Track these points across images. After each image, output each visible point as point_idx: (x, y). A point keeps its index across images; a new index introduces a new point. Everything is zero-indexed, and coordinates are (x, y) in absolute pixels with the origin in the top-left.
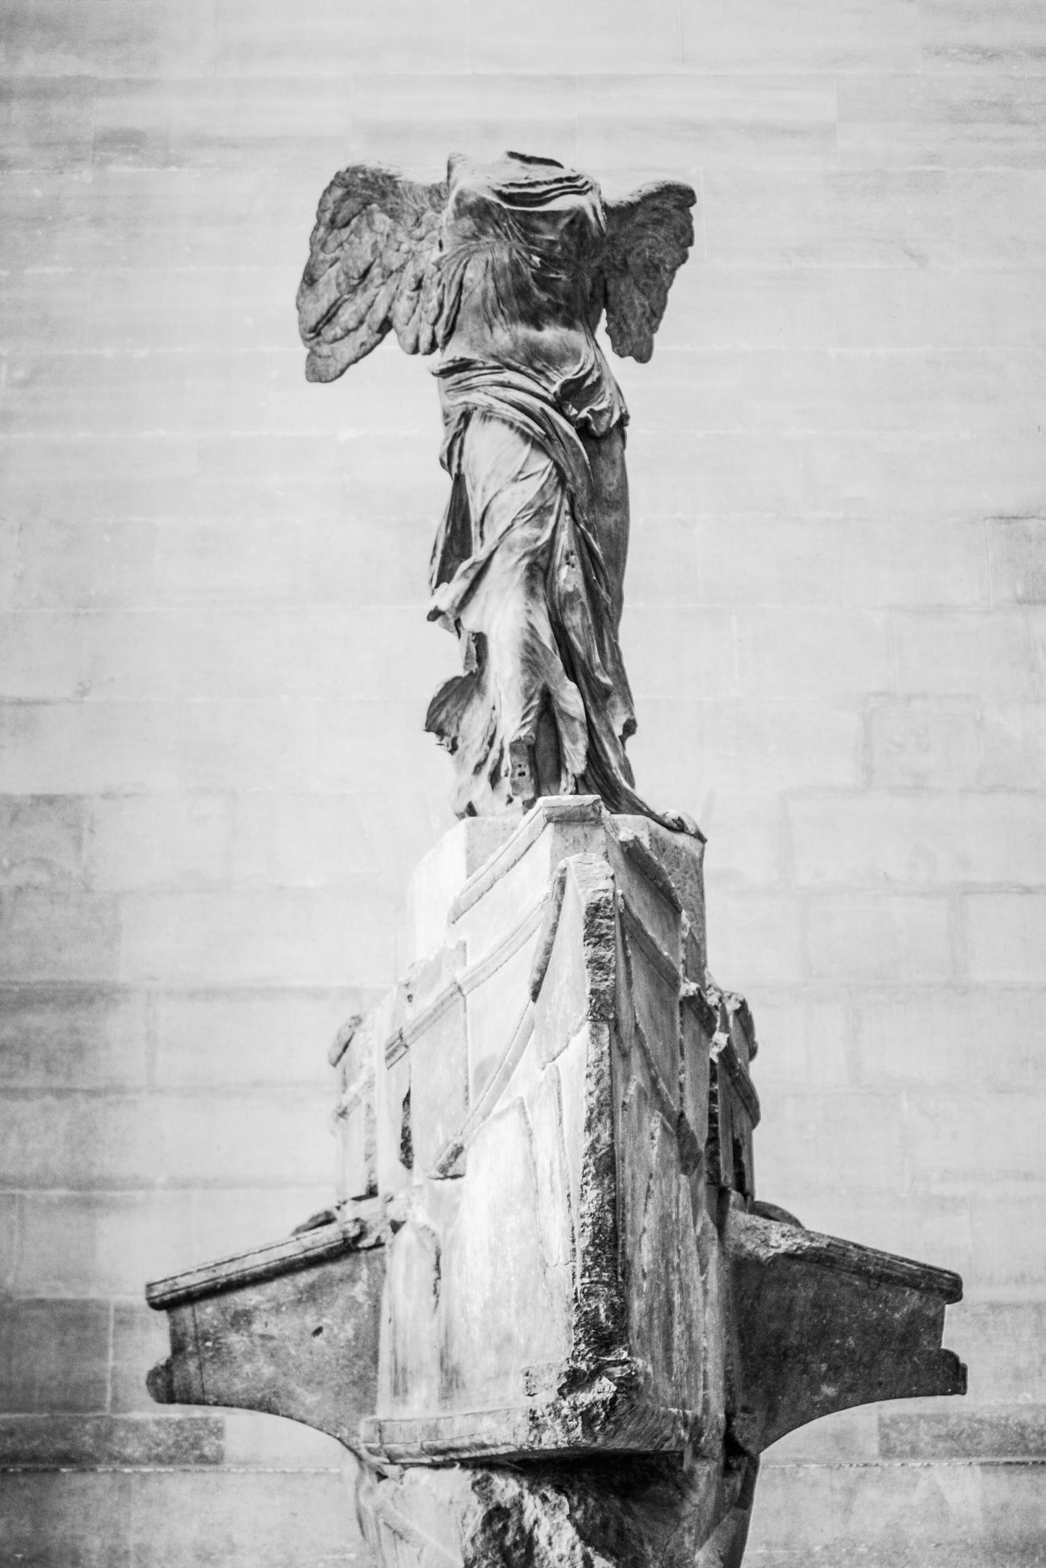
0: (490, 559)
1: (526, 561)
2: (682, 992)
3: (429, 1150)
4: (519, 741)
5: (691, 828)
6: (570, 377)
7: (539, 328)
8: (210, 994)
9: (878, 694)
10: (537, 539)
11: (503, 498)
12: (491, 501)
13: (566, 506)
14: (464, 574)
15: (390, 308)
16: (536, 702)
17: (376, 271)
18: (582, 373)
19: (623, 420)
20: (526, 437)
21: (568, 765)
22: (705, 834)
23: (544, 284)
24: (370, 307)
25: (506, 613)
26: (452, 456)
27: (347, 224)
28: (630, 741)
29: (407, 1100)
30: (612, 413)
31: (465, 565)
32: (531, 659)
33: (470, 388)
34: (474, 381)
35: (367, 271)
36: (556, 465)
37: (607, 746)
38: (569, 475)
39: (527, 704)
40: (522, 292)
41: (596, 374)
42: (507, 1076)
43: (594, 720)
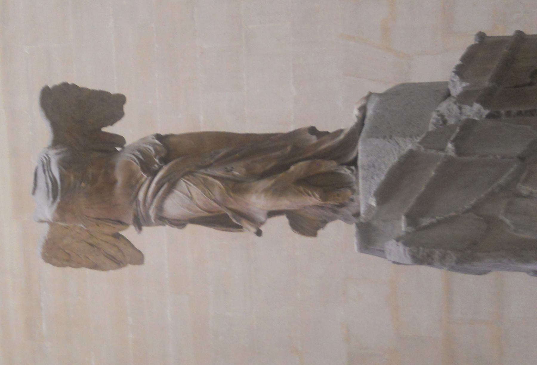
0: (231, 210)
1: (232, 194)
2: (453, 154)
4: (321, 197)
5: (363, 102)
6: (139, 167)
7: (115, 182)
10: (220, 188)
11: (200, 204)
12: (201, 209)
13: (203, 171)
14: (238, 221)
15: (108, 235)
16: (301, 188)
17: (90, 241)
18: (137, 162)
19: (159, 137)
20: (169, 191)
21: (333, 169)
22: (366, 94)
24: (107, 242)
26: (179, 223)
27: (69, 254)
28: (320, 128)
30: (156, 144)
34: (143, 214)
35: (91, 245)
36: (183, 176)
37: (323, 147)
38: (187, 169)
39: (303, 194)
41: (137, 153)
43: (309, 155)
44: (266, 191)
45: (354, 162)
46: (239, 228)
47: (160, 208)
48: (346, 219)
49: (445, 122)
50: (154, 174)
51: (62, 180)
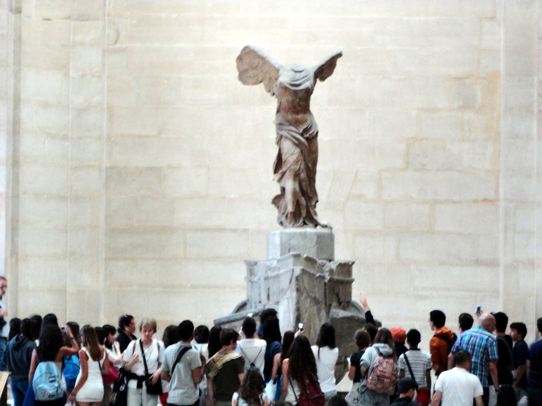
3: (273, 299)
5: (328, 226)
6: (304, 127)
8: (203, 230)
9: (412, 138)
11: (289, 158)
16: (295, 203)
19: (317, 133)
20: (295, 144)
22: (332, 226)
23: (300, 105)
25: (290, 185)
26: (279, 142)
28: (318, 204)
29: (269, 289)
31: (280, 171)
32: (295, 194)
33: (281, 130)
40: (294, 107)
42: (286, 293)
44: (295, 189)
45: (305, 223)
46: (276, 171)
47: (286, 138)
48: (279, 218)
49: (323, 266)
50: (302, 135)
51: (300, 90)
